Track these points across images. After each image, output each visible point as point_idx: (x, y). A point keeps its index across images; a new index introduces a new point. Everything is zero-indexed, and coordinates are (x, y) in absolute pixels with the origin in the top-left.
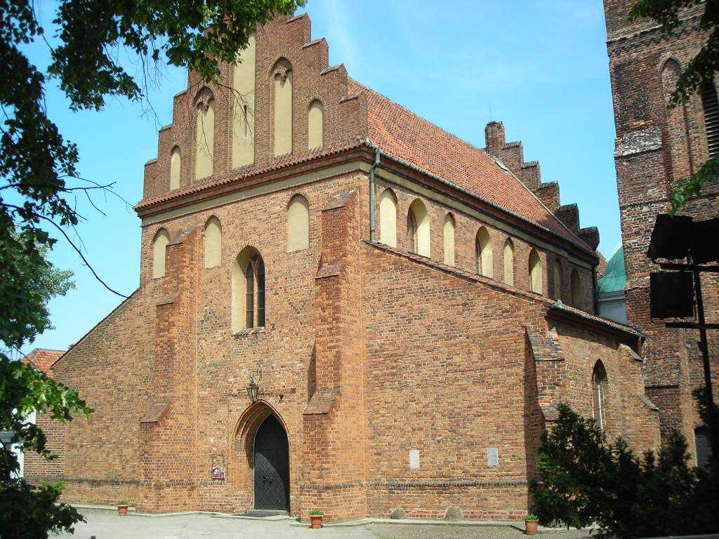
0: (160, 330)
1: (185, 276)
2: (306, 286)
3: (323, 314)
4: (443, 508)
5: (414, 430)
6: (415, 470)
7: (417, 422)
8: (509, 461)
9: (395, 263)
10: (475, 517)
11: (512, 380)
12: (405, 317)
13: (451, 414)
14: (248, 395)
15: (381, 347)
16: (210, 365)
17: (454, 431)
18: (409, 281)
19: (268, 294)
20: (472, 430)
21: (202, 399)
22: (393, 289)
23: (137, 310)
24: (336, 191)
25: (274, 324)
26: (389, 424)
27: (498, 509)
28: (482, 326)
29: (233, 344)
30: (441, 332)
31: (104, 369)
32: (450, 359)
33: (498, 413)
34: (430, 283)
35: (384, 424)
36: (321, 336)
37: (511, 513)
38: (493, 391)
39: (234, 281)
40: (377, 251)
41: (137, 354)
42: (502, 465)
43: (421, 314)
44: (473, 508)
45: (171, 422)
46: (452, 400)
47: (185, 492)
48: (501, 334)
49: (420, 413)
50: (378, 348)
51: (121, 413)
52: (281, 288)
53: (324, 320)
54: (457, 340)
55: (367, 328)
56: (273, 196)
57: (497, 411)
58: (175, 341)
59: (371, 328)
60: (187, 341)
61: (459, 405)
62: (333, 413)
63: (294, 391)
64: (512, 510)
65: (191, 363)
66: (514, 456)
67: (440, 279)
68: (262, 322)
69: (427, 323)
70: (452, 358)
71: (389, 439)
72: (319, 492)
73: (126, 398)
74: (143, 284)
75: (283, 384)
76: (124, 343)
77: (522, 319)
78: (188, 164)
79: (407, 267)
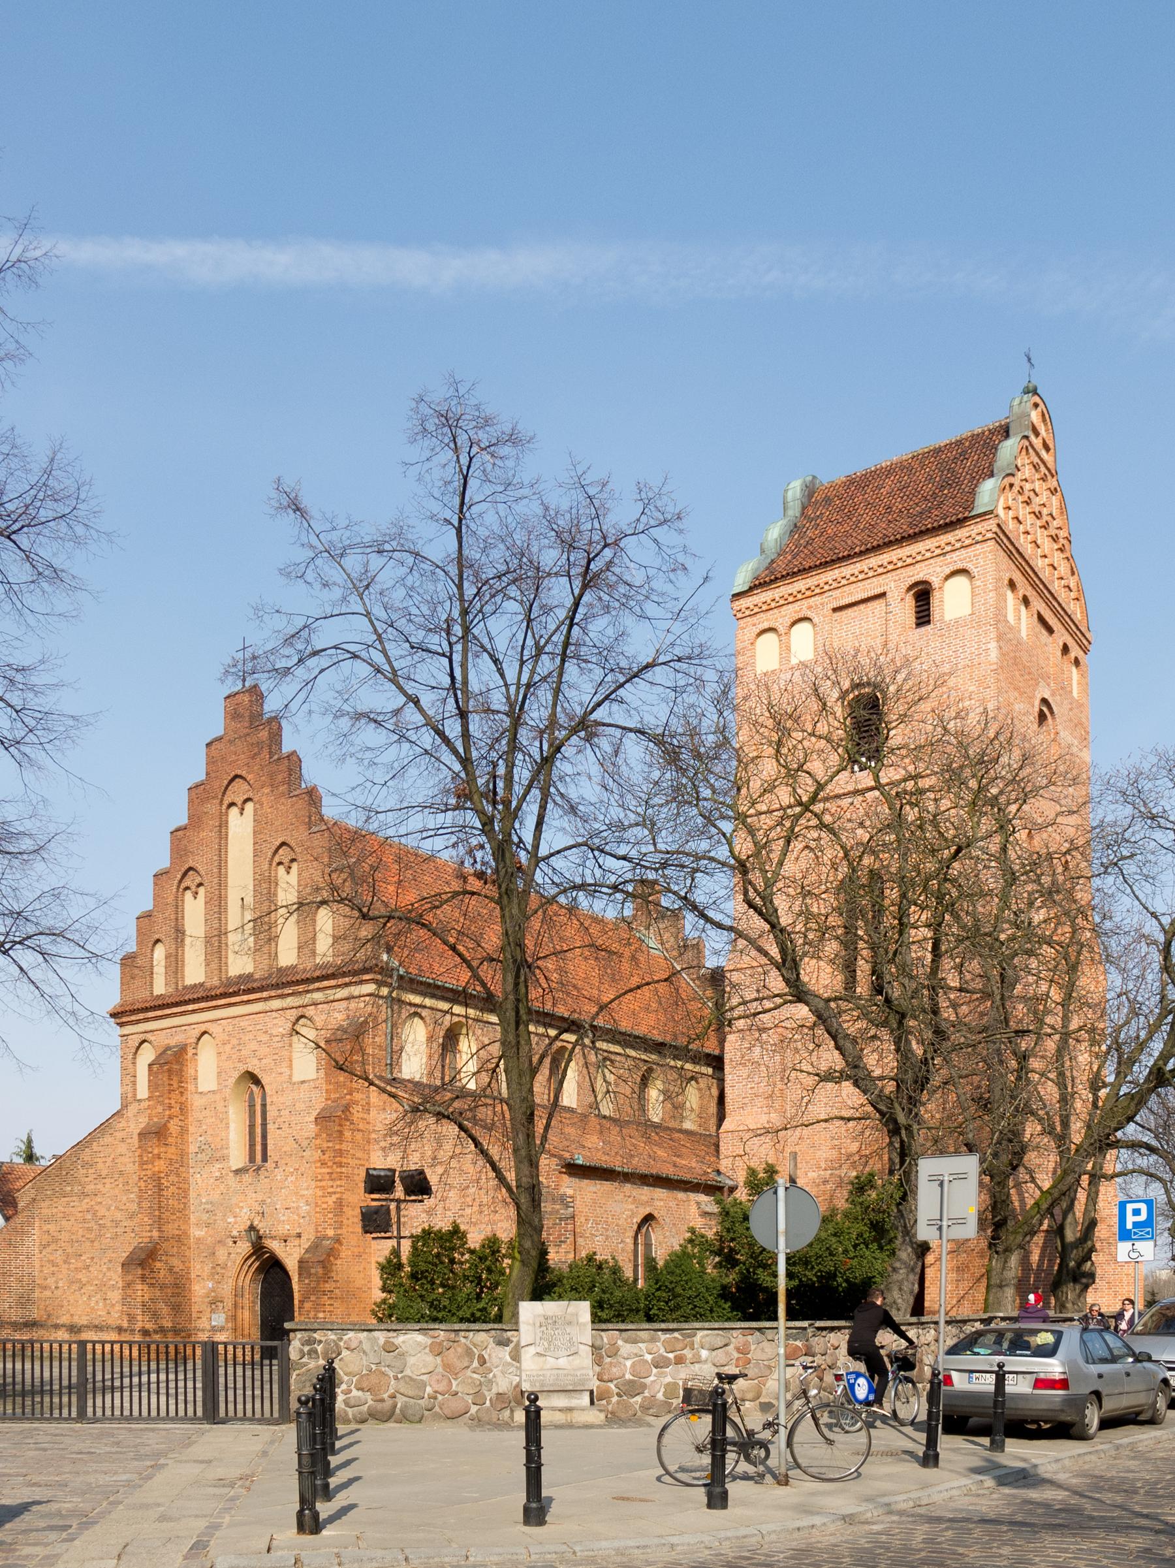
0: (142, 1163)
1: (173, 1102)
19: (271, 1127)
23: (119, 1135)
31: (81, 1201)
39: (231, 1110)
51: (104, 1251)
60: (178, 1175)
68: (265, 1159)
73: (109, 1235)
74: (125, 1106)
76: (104, 1173)
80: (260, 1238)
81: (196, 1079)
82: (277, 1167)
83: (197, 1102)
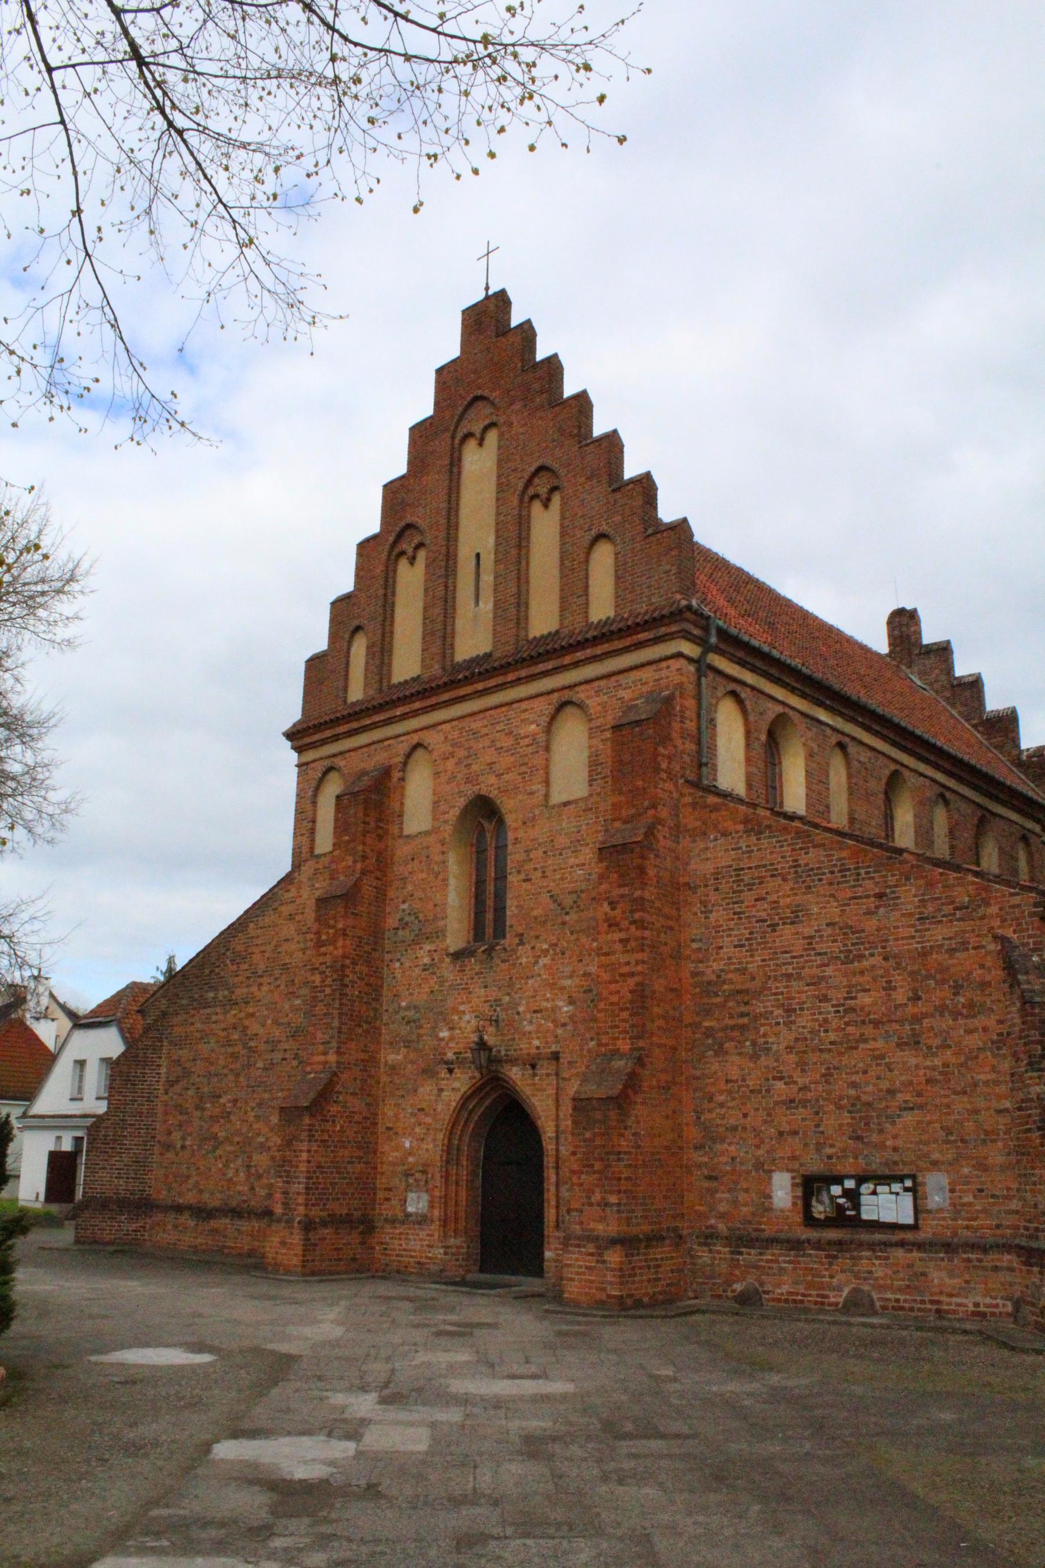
2: (581, 866)
3: (612, 914)
4: (839, 1289)
5: (781, 1134)
6: (782, 1211)
8: (971, 1199)
10: (902, 1308)
11: (975, 1041)
12: (765, 921)
14: (473, 1062)
15: (719, 977)
16: (407, 1008)
17: (859, 1138)
18: (771, 853)
19: (513, 879)
20: (895, 1137)
21: (393, 1069)
22: (743, 869)
24: (636, 694)
25: (522, 935)
26: (732, 1121)
27: (951, 1295)
28: (913, 937)
29: (448, 970)
30: (836, 948)
32: (852, 998)
33: (948, 1106)
34: (812, 857)
35: (725, 1122)
36: (606, 954)
37: (977, 1305)
38: (938, 1062)
40: (712, 799)
41: (282, 987)
42: (957, 1208)
44: (900, 1290)
45: (334, 1109)
46: (854, 1078)
47: (354, 1238)
48: (952, 951)
49: (792, 1101)
50: (713, 977)
52: (535, 869)
53: (612, 924)
54: (865, 963)
55: (693, 941)
56: (524, 705)
57: (945, 1101)
58: (347, 962)
59: (701, 940)
60: (368, 962)
61: (870, 1088)
62: (627, 1096)
64: (979, 1299)
65: (374, 1004)
66: (981, 1191)
67: (831, 849)
68: (500, 931)
69: (808, 931)
70: (854, 998)
71: (733, 1148)
72: (598, 1247)
75: (536, 1043)
79: (769, 827)
80: (491, 1060)
81: (401, 815)
82: (521, 943)
83: (402, 850)
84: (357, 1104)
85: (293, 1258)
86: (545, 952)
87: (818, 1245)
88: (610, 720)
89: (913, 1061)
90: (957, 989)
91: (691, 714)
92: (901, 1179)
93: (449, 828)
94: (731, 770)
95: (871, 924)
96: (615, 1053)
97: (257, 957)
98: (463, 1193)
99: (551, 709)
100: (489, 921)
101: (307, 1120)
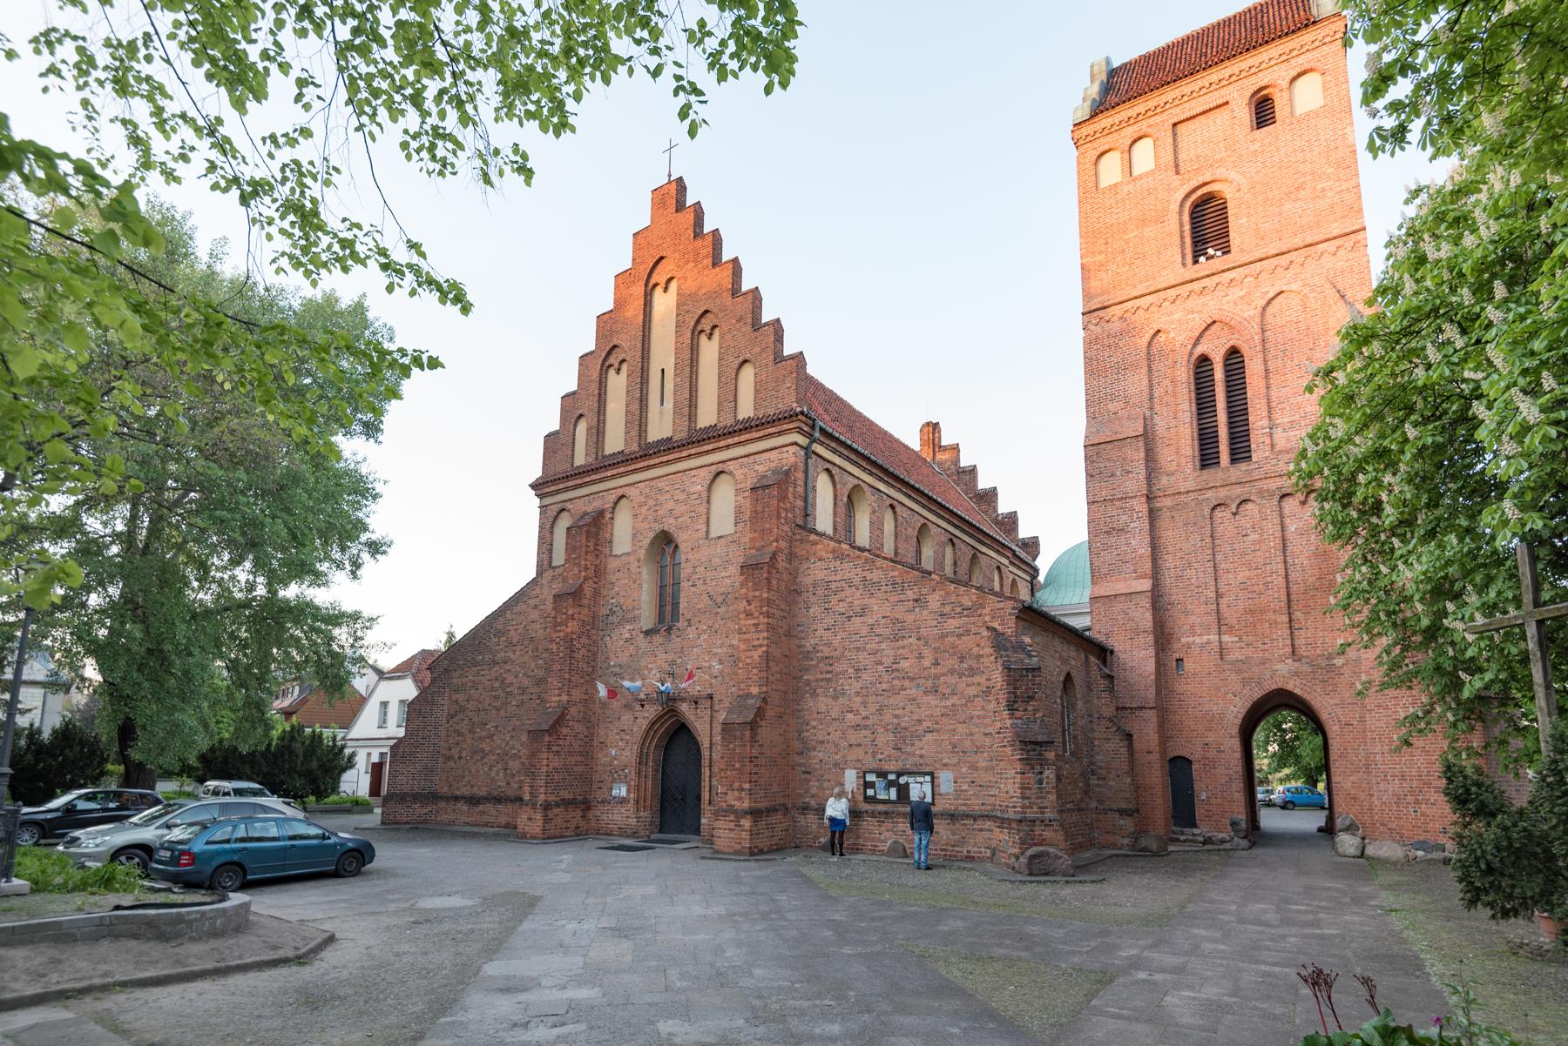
2: (729, 577)
4: (884, 841)
7: (853, 737)
9: (833, 551)
11: (972, 691)
13: (896, 730)
19: (685, 585)
29: (641, 641)
30: (888, 631)
34: (875, 575)
38: (948, 703)
40: (813, 537)
42: (958, 793)
43: (863, 611)
45: (565, 731)
47: (579, 813)
48: (960, 636)
53: (749, 615)
63: (711, 697)
77: (987, 618)
78: (598, 432)
83: (613, 564)
84: (580, 728)
85: (536, 827)
86: (705, 632)
87: (873, 814)
88: (749, 485)
89: (933, 703)
90: (962, 659)
91: (801, 483)
92: (925, 774)
93: (643, 552)
94: (824, 519)
95: (910, 618)
96: (749, 695)
97: (512, 633)
98: (650, 783)
99: (711, 476)
100: (668, 614)
101: (547, 738)
